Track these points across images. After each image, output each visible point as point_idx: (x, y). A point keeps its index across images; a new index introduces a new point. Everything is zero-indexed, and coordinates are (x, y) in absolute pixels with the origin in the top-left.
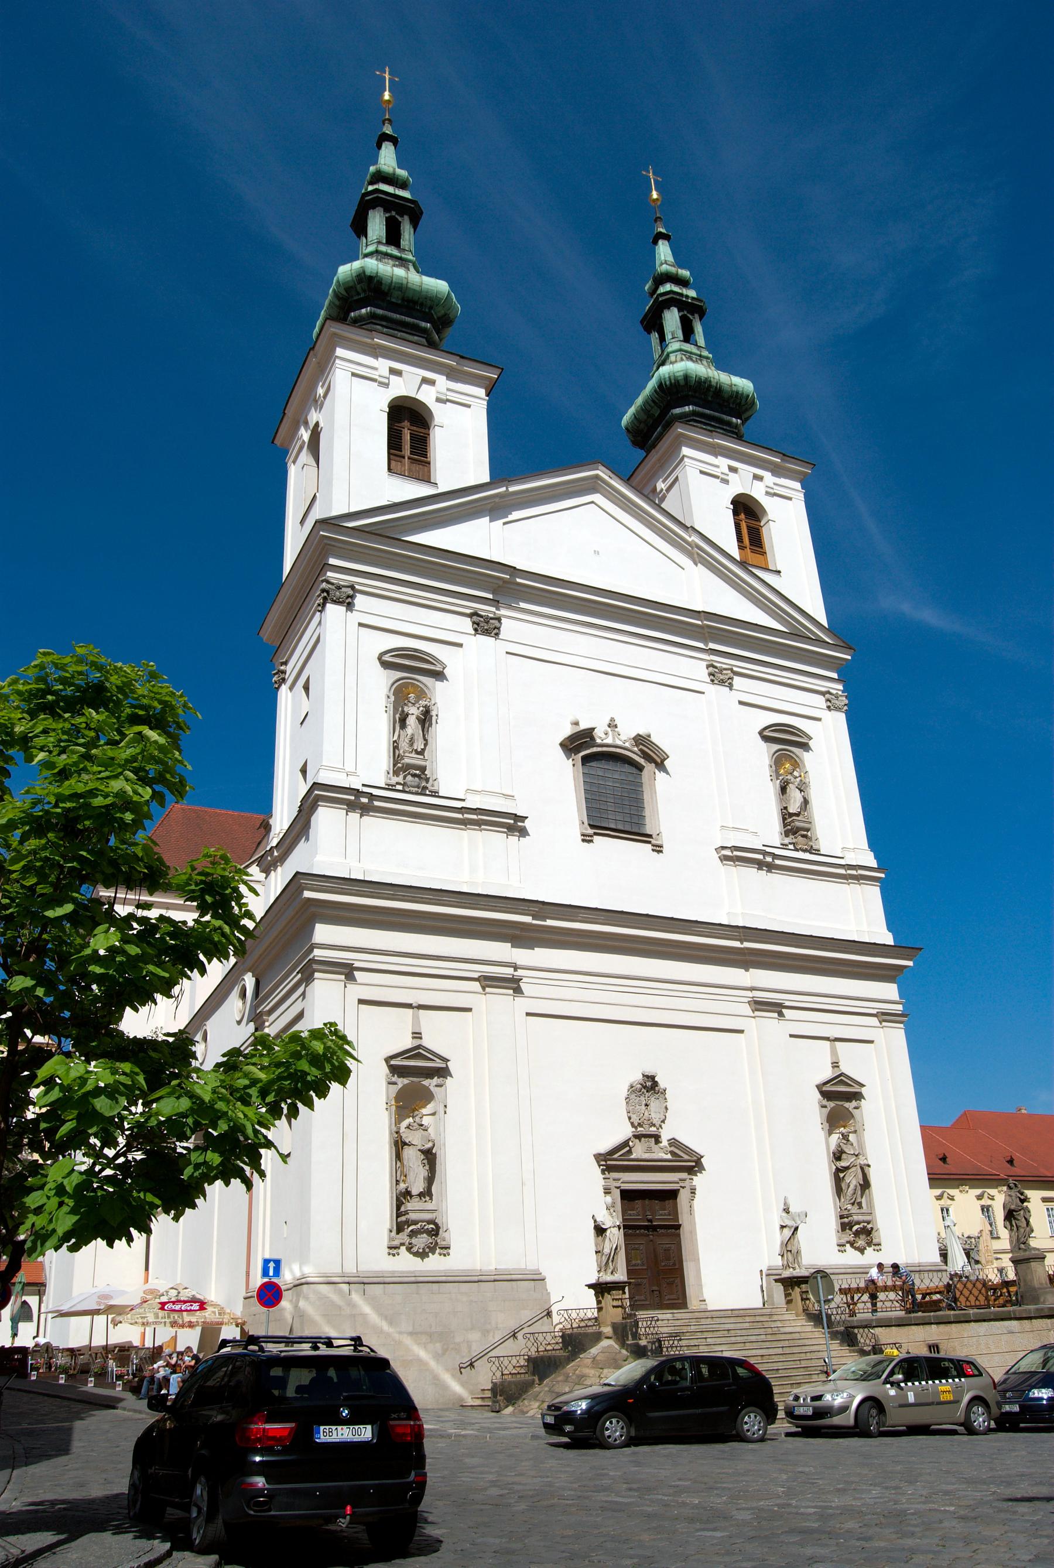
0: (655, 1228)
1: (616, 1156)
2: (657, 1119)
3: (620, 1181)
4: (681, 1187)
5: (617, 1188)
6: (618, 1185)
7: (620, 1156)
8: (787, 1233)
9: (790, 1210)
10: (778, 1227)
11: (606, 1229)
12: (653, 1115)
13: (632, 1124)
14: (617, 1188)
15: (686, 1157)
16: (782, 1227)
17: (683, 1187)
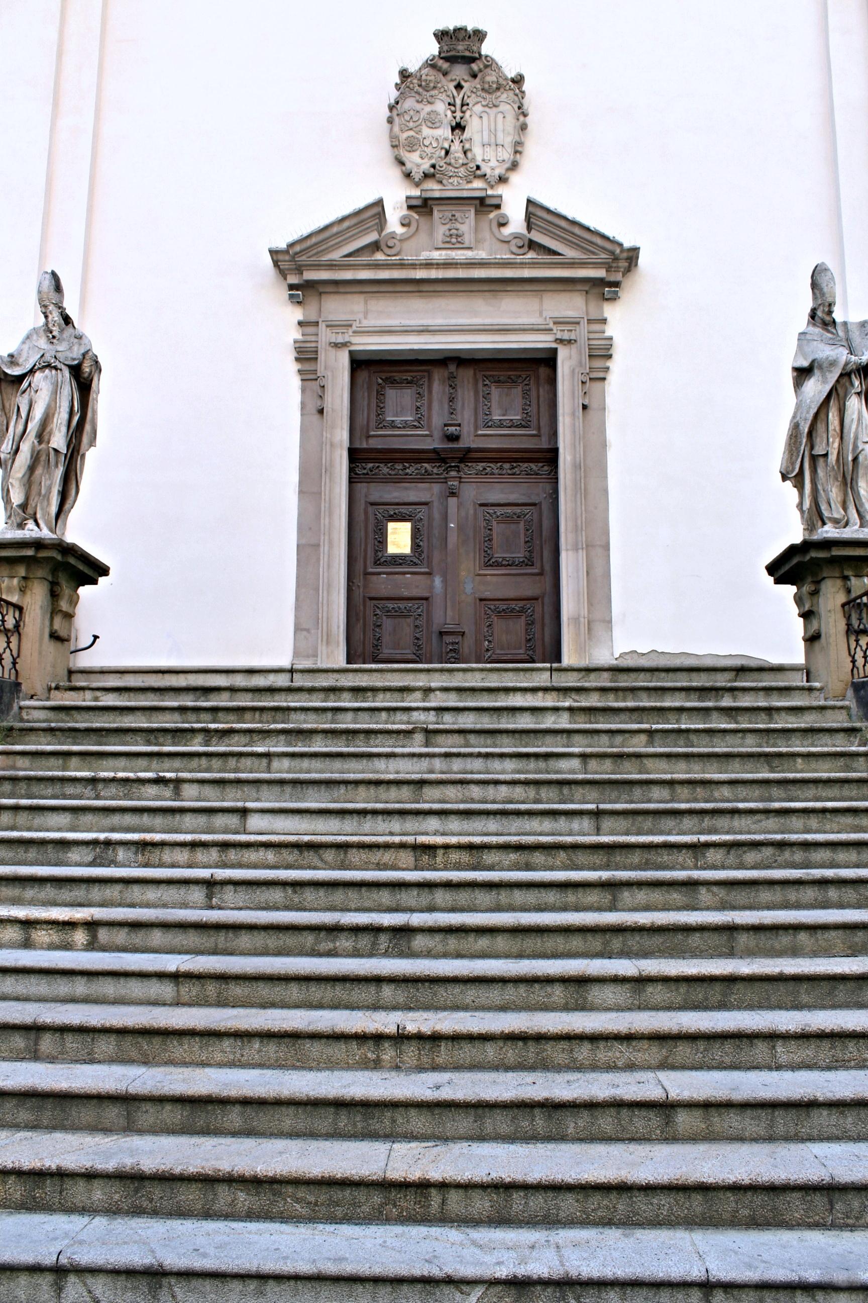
0: (467, 456)
1: (336, 255)
2: (493, 163)
3: (350, 331)
4: (560, 341)
5: (336, 345)
6: (340, 339)
7: (349, 255)
8: (815, 388)
9: (838, 315)
10: (788, 377)
11: (20, 379)
12: (478, 153)
13: (408, 175)
14: (336, 345)
15: (570, 253)
16: (802, 374)
17: (569, 342)
